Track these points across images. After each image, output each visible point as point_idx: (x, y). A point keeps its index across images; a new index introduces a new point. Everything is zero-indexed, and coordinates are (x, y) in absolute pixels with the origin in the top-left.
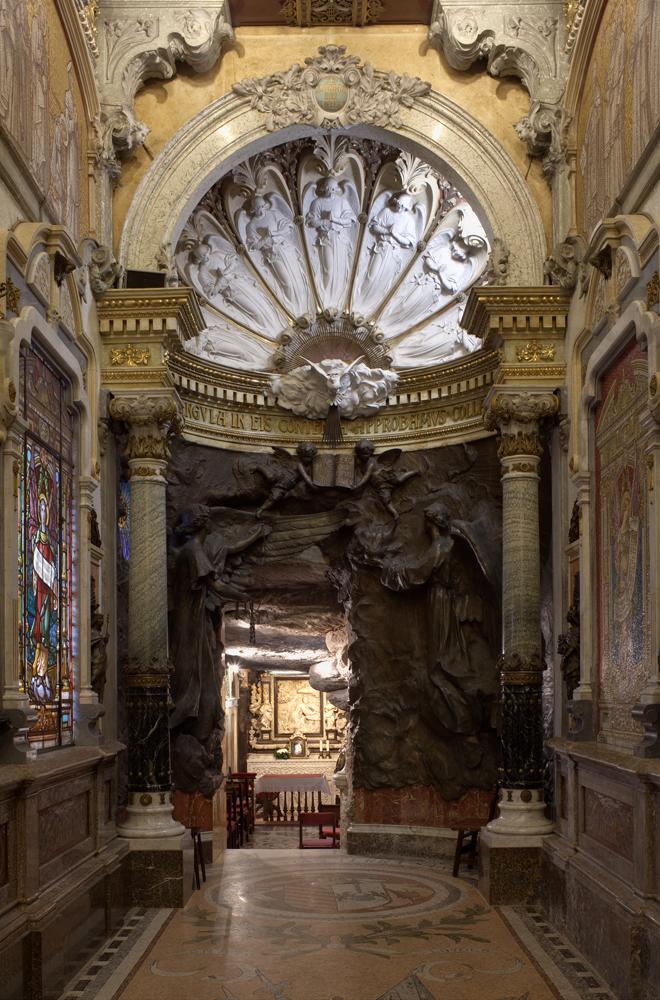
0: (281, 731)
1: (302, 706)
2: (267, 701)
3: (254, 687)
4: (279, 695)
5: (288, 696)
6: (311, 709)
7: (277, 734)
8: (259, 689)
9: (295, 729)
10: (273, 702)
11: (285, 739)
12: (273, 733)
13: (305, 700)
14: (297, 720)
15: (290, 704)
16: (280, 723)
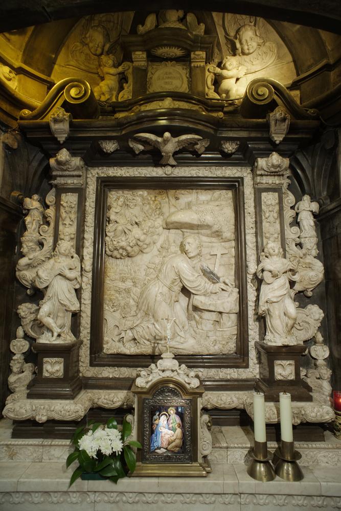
0: (111, 345)
1: (183, 265)
2: (66, 245)
3: (32, 203)
4: (110, 228)
5: (137, 232)
6: (211, 276)
7: (97, 355)
8: (51, 212)
9: (156, 339)
10: (88, 251)
11: (125, 372)
12: (85, 353)
13: (191, 247)
14: (163, 310)
15: (143, 260)
16: (111, 317)
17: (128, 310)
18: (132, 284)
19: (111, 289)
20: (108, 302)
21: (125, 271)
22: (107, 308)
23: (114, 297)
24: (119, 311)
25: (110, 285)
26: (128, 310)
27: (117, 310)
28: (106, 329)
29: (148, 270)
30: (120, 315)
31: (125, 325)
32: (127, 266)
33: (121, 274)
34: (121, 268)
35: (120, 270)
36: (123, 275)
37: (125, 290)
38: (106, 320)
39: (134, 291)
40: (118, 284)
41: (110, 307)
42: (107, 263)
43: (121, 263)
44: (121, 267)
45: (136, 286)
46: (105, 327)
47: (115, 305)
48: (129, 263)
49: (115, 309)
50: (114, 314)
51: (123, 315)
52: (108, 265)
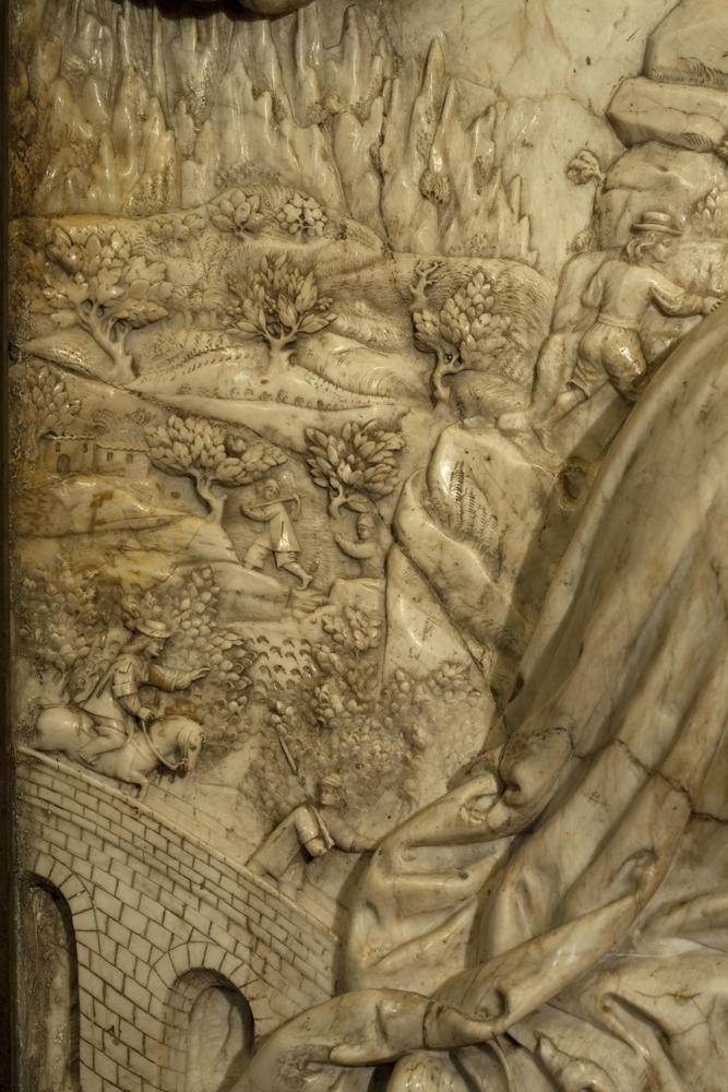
17: (379, 746)
18: (407, 368)
19: (116, 443)
20: (65, 638)
21: (309, 191)
22: (60, 723)
23: (157, 567)
24: (236, 765)
25: (92, 393)
26: (379, 746)
27: (214, 750)
28: (57, 1020)
29: (636, 169)
30: (251, 824)
31: (342, 983)
32: (329, 122)
33: (241, 229)
34: (242, 153)
35: (224, 181)
36: (270, 243)
37: (308, 453)
38: (55, 894)
39: (444, 470)
40: (204, 373)
41: (105, 706)
42: (44, 70)
43: (237, 86)
44: (239, 140)
45: (461, 408)
46: (42, 988)
47: (175, 672)
48: (354, 82)
49: (189, 731)
50: (169, 806)
51: (306, 822)
52: (61, 98)
